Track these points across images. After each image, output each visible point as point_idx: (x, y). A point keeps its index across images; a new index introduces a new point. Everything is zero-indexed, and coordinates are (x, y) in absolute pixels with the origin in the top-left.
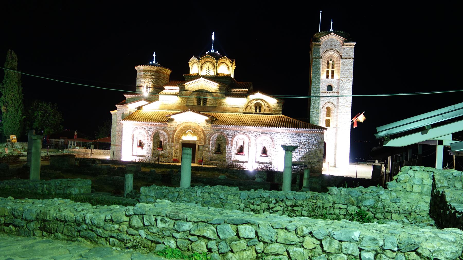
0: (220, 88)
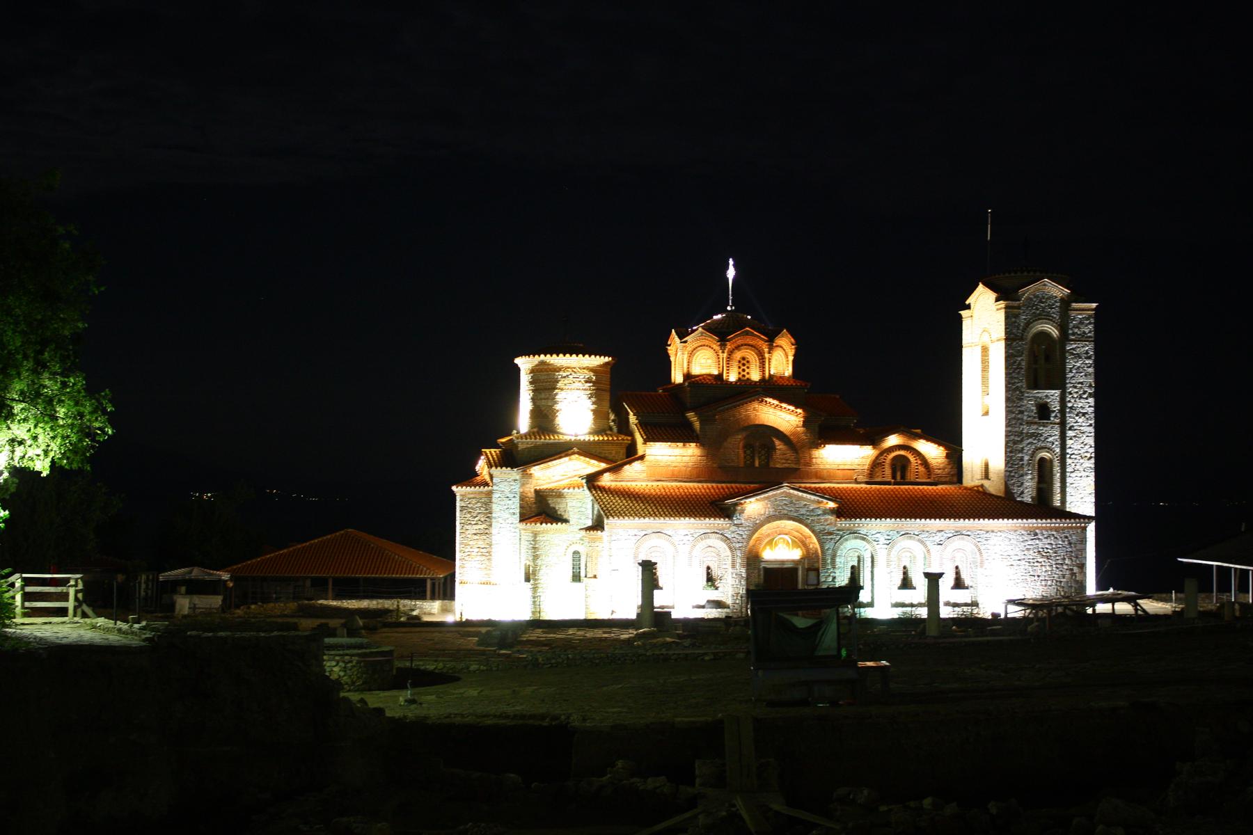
0: (805, 424)
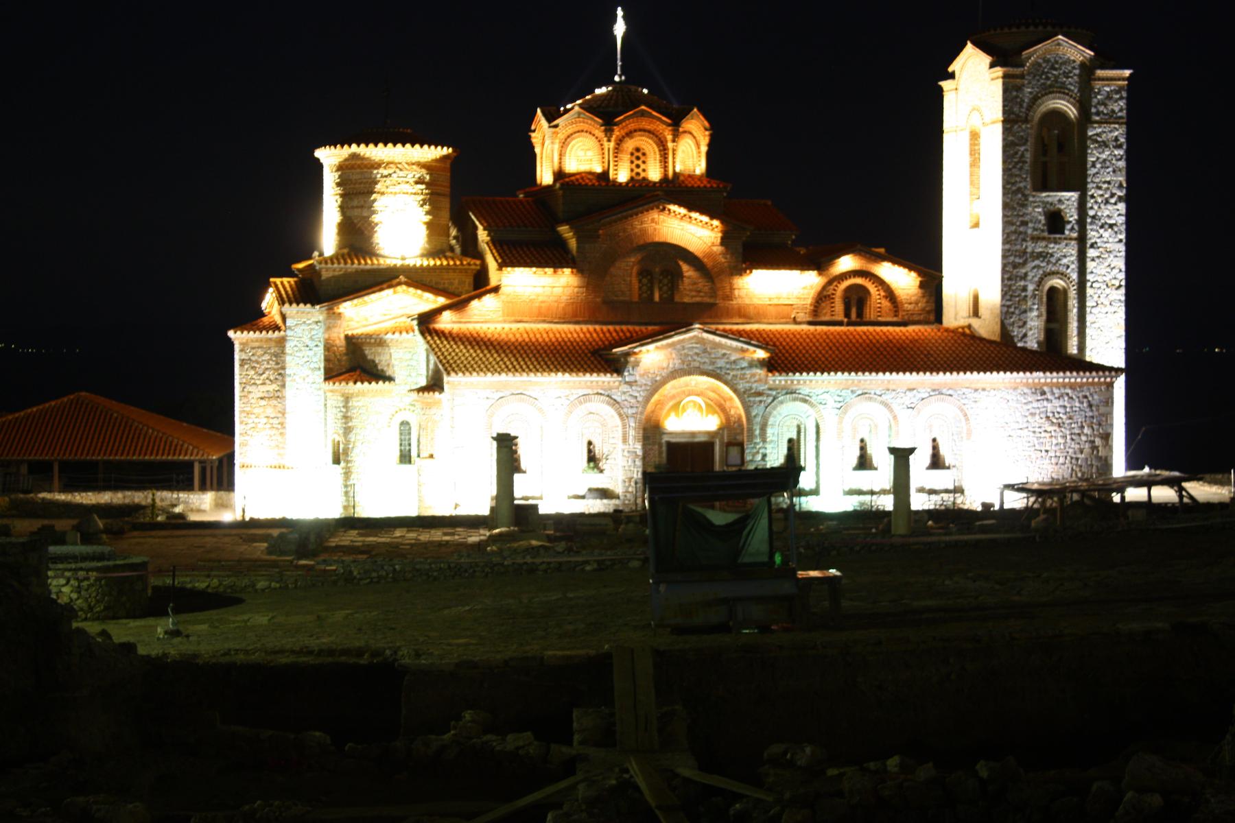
0: (725, 240)
